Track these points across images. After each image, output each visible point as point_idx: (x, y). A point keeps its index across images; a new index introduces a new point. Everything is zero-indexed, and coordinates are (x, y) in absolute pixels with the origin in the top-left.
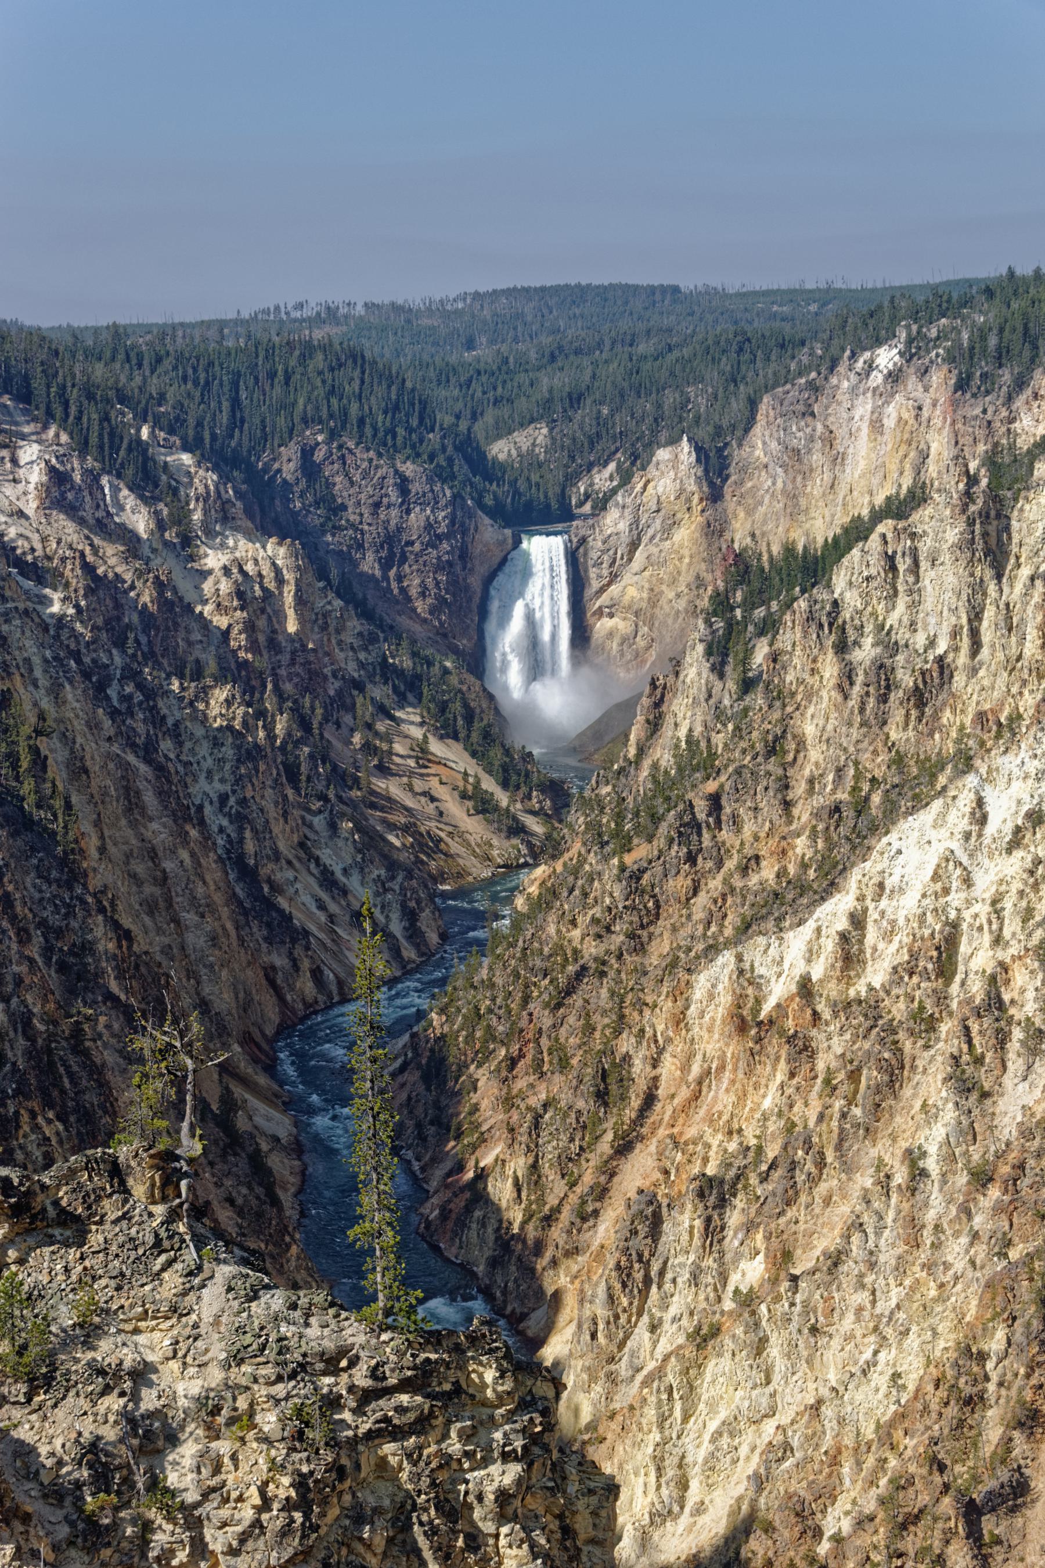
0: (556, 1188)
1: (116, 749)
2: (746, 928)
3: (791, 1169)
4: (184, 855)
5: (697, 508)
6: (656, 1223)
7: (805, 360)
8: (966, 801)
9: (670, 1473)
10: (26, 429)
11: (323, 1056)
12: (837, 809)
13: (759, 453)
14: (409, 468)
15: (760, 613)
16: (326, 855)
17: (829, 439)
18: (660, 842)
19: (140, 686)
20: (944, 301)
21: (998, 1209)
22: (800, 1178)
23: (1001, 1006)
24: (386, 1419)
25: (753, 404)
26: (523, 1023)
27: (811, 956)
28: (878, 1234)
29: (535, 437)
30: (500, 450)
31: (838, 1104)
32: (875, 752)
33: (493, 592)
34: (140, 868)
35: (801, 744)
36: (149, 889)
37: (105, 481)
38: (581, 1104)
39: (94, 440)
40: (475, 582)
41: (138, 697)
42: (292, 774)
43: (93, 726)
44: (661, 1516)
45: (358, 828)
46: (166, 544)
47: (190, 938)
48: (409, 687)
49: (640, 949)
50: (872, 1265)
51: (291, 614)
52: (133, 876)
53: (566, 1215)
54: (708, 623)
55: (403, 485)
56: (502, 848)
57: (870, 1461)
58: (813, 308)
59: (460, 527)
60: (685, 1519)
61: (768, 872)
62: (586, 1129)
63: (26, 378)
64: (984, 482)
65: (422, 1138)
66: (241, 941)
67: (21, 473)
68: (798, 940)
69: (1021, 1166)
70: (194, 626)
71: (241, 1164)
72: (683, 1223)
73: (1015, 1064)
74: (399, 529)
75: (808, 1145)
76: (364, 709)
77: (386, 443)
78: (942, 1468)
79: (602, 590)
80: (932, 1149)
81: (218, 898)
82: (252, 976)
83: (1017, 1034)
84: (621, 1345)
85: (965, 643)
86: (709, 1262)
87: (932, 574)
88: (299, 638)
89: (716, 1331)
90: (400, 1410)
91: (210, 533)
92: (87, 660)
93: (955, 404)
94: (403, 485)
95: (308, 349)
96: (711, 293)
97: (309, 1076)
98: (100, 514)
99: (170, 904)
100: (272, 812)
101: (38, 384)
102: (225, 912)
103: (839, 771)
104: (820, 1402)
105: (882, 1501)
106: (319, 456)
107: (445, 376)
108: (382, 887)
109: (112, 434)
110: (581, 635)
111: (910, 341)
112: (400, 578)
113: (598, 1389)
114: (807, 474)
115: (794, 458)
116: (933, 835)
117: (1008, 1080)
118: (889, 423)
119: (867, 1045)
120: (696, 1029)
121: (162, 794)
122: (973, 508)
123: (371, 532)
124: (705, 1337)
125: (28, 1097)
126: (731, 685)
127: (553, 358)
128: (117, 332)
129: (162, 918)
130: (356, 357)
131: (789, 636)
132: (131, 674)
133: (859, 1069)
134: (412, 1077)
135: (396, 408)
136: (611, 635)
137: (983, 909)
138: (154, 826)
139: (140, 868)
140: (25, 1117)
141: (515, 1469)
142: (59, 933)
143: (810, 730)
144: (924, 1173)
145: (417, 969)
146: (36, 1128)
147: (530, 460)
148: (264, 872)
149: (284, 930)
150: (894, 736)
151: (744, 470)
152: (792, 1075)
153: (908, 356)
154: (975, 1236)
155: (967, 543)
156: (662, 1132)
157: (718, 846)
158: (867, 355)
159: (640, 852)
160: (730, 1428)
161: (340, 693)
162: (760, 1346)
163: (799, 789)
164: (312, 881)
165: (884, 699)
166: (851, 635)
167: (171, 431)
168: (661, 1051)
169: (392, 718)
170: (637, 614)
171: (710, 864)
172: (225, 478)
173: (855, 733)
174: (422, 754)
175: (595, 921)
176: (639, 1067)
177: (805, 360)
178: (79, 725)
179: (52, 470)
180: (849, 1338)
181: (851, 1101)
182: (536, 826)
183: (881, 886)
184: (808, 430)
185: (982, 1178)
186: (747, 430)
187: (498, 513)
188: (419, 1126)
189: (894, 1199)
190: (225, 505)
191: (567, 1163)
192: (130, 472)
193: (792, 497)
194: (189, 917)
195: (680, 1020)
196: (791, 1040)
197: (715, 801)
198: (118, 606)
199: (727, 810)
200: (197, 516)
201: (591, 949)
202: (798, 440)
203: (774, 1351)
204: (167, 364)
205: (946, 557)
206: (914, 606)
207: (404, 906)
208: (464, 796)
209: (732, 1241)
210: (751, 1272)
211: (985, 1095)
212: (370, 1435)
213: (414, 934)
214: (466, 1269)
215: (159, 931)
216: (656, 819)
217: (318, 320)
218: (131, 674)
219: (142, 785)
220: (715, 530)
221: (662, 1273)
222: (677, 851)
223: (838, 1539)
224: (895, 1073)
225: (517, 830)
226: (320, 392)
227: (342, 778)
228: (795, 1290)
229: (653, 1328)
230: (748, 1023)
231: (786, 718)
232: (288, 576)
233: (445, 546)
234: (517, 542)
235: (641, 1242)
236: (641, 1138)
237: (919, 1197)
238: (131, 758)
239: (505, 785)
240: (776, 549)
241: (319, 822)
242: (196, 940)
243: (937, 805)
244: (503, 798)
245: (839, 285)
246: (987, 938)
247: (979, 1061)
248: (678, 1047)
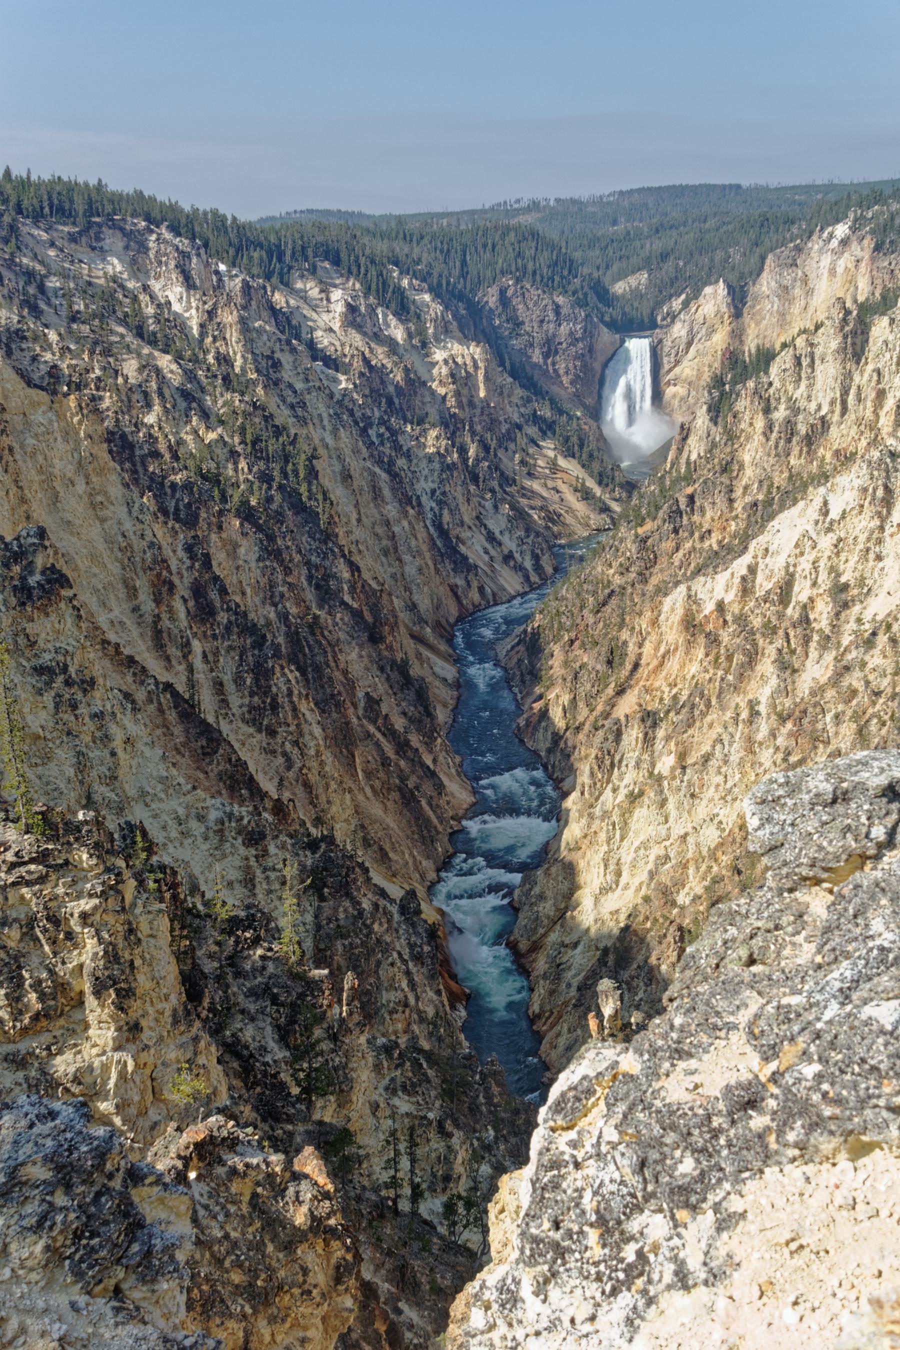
0: (583, 712)
1: (368, 464)
2: (698, 571)
3: (692, 708)
4: (405, 524)
5: (727, 322)
6: (618, 735)
7: (795, 231)
8: (818, 502)
9: (612, 867)
10: (338, 282)
11: (480, 635)
12: (755, 504)
13: (764, 288)
14: (560, 300)
16: (491, 524)
17: (805, 280)
18: (659, 522)
19: (388, 429)
20: (875, 194)
21: (790, 734)
22: (697, 713)
23: (808, 621)
24: (22, 877)
25: (763, 259)
26: (579, 621)
27: (727, 589)
28: (730, 745)
30: (620, 288)
31: (720, 673)
32: (782, 472)
33: (607, 372)
34: (380, 530)
35: (741, 467)
36: (385, 542)
37: (379, 311)
38: (599, 667)
39: (374, 287)
40: (597, 366)
41: (387, 435)
42: (475, 479)
43: (356, 451)
44: (605, 890)
45: (512, 508)
46: (413, 346)
47: (407, 569)
48: (547, 428)
49: (645, 581)
50: (726, 762)
51: (482, 386)
52: (377, 535)
53: (587, 727)
54: (710, 393)
55: (557, 309)
56: (596, 520)
57: (704, 867)
58: (820, 196)
59: (589, 333)
60: (619, 892)
61: (713, 542)
62: (601, 681)
63: (338, 253)
64: (855, 313)
65: (523, 682)
66: (437, 571)
67: (332, 306)
68: (722, 578)
69: (805, 712)
70: (427, 393)
71: (411, 695)
72: (633, 734)
73: (813, 654)
74: (554, 335)
75: (702, 695)
76: (522, 441)
77: (548, 285)
78: (739, 872)
79: (670, 370)
80: (764, 700)
81: (424, 548)
82: (443, 591)
83: (816, 638)
84: (597, 799)
85: (838, 408)
86: (646, 757)
87: (822, 367)
88: (486, 401)
89: (641, 794)
90: (29, 872)
91: (438, 340)
92: (358, 414)
93: (873, 259)
94: (557, 309)
95: (507, 230)
96: (758, 189)
97: (471, 645)
98: (376, 330)
99: (396, 551)
100: (461, 499)
101: (343, 255)
102: (428, 555)
103: (761, 481)
104: (686, 834)
105: (707, 889)
106: (510, 293)
107: (593, 242)
108: (521, 542)
109: (384, 283)
110: (657, 396)
111: (856, 220)
112: (554, 364)
113: (584, 821)
114: (791, 302)
115: (785, 291)
116: (798, 521)
117: (808, 663)
118: (840, 270)
119: (738, 641)
120: (663, 628)
121: (393, 489)
122: (847, 329)
123: (538, 337)
124: (634, 798)
125: (279, 658)
127: (657, 231)
128: (400, 220)
129: (392, 558)
130: (534, 235)
132: (383, 422)
133: (732, 655)
134: (521, 648)
135: (556, 264)
136: (674, 396)
137: (808, 566)
138: (389, 507)
139: (380, 530)
140: (277, 669)
141: (96, 901)
142: (317, 568)
143: (747, 458)
144: (758, 713)
145: (539, 587)
146: (284, 675)
147: (636, 293)
148: (453, 533)
149: (463, 565)
150: (792, 462)
151: (755, 299)
152: (707, 655)
153: (854, 229)
154: (777, 749)
156: (642, 683)
157: (692, 524)
158: (830, 229)
159: (649, 526)
160: (646, 845)
161: (508, 431)
162: (663, 803)
163: (739, 492)
164: (482, 538)
165: (789, 441)
166: (773, 403)
167: (424, 280)
168: (644, 640)
169: (538, 446)
170: (690, 384)
171: (686, 534)
172: (447, 308)
173: (772, 460)
174: (554, 467)
175: (621, 565)
176: (632, 648)
177: (795, 231)
178: (348, 452)
179: (348, 305)
180: (711, 800)
181: (727, 671)
182: (616, 507)
183: (767, 550)
185: (783, 719)
186: (759, 275)
187: (613, 326)
188: (522, 675)
189: (741, 726)
190: (446, 324)
191: (590, 700)
192: (393, 305)
193: (782, 315)
194: (407, 558)
195: (655, 622)
196: (708, 635)
197: (691, 499)
198: (383, 382)
199: (698, 504)
200: (431, 331)
201: (618, 580)
202: (787, 280)
203: (671, 806)
204: (426, 240)
205: (829, 358)
206: (810, 386)
207: (533, 552)
208: (576, 490)
209: (659, 745)
210: (666, 764)
211: (795, 671)
212: (14, 884)
213: (538, 567)
214: (536, 753)
215: (390, 565)
216: (658, 508)
217: (528, 210)
218: (383, 422)
219: (382, 485)
220: (737, 335)
221: (620, 761)
222: (669, 527)
223: (682, 908)
224: (752, 657)
225: (605, 509)
226: (512, 255)
227: (507, 480)
228: (684, 774)
229: (615, 790)
230: (691, 625)
231: (733, 452)
232: (481, 364)
233: (580, 345)
234: (623, 342)
235: (610, 745)
236: (631, 687)
237: (754, 726)
238: (377, 470)
239: (600, 483)
240: (753, 351)
241: (488, 505)
242: (410, 570)
243: (801, 504)
244: (598, 491)
245: (836, 181)
246: (809, 583)
247: (793, 652)
248: (653, 637)
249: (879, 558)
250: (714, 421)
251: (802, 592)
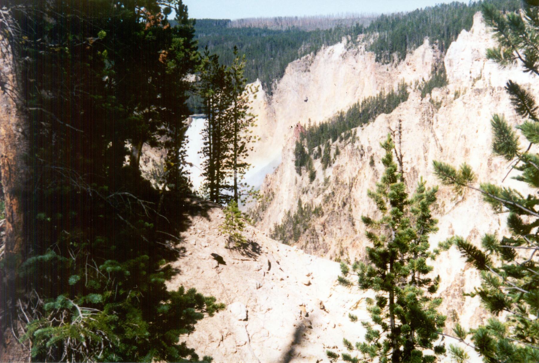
85: (422, 162)
155: (422, 123)
184: (308, 77)
250: (299, 172)
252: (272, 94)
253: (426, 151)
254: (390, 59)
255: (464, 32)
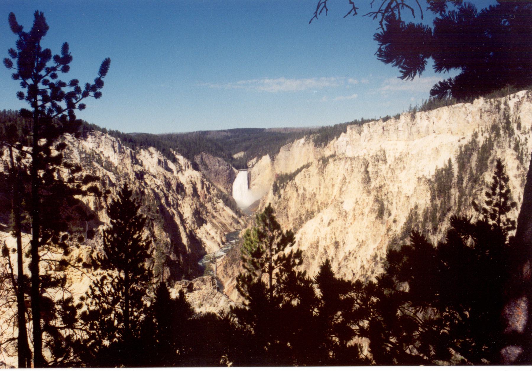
14: (220, 159)
15: (282, 185)
25: (279, 149)
29: (241, 154)
30: (235, 156)
85: (318, 190)
126: (277, 198)
131: (288, 188)
147: (241, 158)
153: (306, 141)
155: (318, 173)
220: (273, 169)
244: (236, 217)
249: (347, 233)
250: (274, 194)
251: (322, 244)
252: (274, 161)
253: (320, 185)
254: (320, 145)
255: (343, 134)
